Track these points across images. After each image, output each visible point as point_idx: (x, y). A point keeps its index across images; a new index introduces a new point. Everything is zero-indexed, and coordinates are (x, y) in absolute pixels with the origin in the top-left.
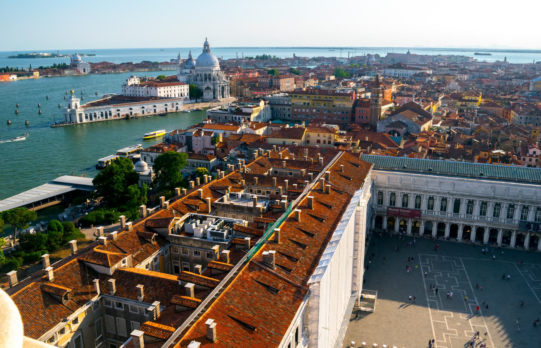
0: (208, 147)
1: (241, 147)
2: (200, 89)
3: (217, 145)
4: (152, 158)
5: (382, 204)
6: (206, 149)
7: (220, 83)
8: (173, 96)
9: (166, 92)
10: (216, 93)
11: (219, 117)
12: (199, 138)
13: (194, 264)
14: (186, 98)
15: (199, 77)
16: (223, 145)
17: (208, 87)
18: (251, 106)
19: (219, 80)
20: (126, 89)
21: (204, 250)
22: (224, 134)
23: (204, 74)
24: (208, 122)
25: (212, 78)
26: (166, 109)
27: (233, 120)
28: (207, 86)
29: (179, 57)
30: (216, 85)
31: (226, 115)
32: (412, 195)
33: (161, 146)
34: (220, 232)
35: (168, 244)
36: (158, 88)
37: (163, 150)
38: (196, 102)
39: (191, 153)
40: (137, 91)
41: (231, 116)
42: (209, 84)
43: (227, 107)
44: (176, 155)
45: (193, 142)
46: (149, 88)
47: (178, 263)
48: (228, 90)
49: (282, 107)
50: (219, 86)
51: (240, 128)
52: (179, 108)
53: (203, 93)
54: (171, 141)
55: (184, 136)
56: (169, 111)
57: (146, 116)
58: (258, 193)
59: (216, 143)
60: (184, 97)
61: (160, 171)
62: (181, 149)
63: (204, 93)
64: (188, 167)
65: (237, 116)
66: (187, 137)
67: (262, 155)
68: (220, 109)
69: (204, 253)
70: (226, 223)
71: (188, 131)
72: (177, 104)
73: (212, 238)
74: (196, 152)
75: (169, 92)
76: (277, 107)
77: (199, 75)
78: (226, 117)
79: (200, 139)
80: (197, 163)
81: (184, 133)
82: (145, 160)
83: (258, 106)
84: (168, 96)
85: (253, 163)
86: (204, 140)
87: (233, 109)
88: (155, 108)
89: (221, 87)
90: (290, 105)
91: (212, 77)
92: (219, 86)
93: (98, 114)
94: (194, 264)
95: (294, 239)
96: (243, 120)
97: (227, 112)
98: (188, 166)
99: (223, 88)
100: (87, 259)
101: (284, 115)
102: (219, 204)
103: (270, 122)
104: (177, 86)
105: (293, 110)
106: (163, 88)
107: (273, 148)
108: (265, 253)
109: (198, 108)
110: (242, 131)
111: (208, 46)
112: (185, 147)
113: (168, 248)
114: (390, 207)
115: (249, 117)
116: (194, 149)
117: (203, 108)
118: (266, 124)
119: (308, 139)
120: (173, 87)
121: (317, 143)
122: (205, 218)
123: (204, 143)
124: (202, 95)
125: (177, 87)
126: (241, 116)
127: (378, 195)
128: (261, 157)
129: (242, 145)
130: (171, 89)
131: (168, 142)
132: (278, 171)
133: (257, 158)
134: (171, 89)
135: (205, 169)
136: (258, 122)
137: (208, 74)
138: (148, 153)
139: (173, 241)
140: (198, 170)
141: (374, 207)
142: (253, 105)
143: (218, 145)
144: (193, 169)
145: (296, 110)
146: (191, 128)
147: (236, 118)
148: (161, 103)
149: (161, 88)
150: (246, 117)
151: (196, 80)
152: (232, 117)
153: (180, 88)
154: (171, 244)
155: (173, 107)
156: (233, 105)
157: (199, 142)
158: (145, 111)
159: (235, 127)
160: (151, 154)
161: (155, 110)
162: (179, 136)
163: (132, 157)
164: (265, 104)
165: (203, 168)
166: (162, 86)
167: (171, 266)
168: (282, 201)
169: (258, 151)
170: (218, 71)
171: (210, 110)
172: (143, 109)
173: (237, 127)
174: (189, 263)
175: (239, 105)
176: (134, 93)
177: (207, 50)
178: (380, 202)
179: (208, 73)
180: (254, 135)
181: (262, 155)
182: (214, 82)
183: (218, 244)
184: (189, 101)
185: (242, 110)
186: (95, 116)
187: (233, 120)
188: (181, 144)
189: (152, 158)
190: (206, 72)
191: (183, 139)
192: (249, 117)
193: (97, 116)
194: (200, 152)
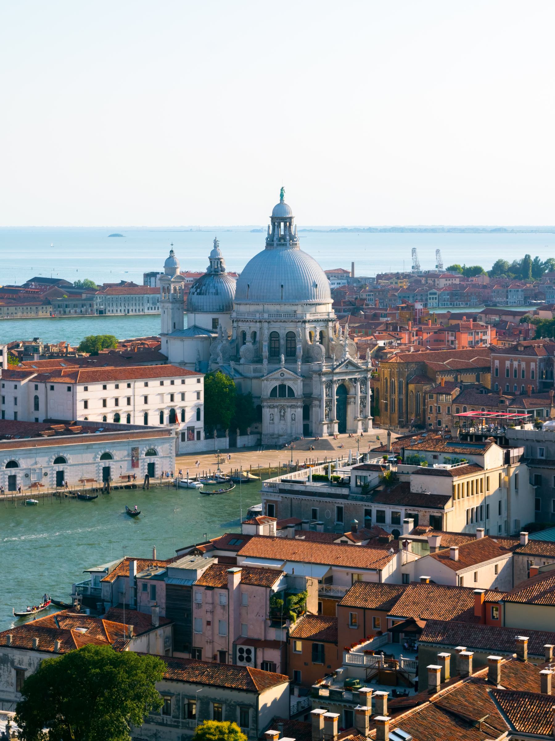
0: (256, 637)
1: (395, 640)
2: (249, 397)
3: (293, 626)
4: (20, 672)
7: (332, 373)
8: (138, 421)
9: (111, 403)
10: (314, 410)
11: (314, 512)
12: (222, 596)
14: (191, 429)
15: (249, 345)
16: (321, 626)
17: (282, 387)
18: (449, 467)
19: (329, 358)
22: (328, 580)
23: (266, 333)
24: (262, 530)
25: (300, 353)
26: (107, 471)
27: (368, 523)
28: (277, 384)
30: (315, 377)
31: (341, 502)
33: (63, 625)
36: (80, 389)
37: (69, 642)
38: (233, 447)
39: (186, 656)
41: (363, 505)
42: (289, 374)
43: (351, 467)
44: (116, 662)
45: (196, 613)
46: (41, 386)
48: (364, 399)
50: (329, 385)
51: (395, 558)
52: (158, 472)
53: (259, 409)
54: (107, 606)
55: (161, 587)
57: (25, 502)
59: (291, 619)
61: (46, 731)
62: (144, 639)
63: (266, 412)
64: (168, 719)
65: (388, 510)
66: (167, 585)
67: (464, 676)
68: (316, 478)
71: (174, 565)
72: (152, 453)
74: (207, 654)
75: (123, 402)
77: (249, 338)
78: (340, 510)
79: (224, 600)
80: (205, 702)
81: (160, 571)
83: (479, 467)
84: (117, 418)
85: (422, 706)
86: (240, 604)
87: (373, 477)
88: (60, 467)
89: (335, 387)
91: (299, 346)
92: (329, 385)
96: (411, 526)
97: (345, 491)
98: (166, 712)
99: (343, 390)
103: (526, 538)
104: (158, 383)
106: (100, 387)
107: (518, 647)
109: (236, 472)
110: (404, 570)
111: (288, 221)
112: (160, 631)
115: (436, 513)
116: (197, 641)
117: (254, 473)
118: (506, 544)
120: (139, 385)
123: (239, 616)
124: (259, 418)
125: (154, 384)
126: (402, 510)
128: (459, 684)
129: (396, 631)
130: (129, 392)
133: (444, 684)
134: (129, 392)
135: (235, 726)
136: (474, 536)
137: (283, 333)
138: (8, 651)
140: (207, 731)
142: (453, 462)
143: (300, 628)
144: (186, 726)
146: (192, 553)
147: (381, 517)
148: (88, 447)
149: (90, 387)
150: (425, 514)
151: (237, 359)
152: (368, 513)
153: (167, 388)
155: (134, 464)
156: (374, 462)
157: (219, 610)
158: (18, 479)
159: (375, 554)
160: (17, 656)
161: (60, 475)
162: (140, 585)
164: (507, 460)
165: (225, 725)
166: (94, 378)
169: (453, 659)
170: (327, 321)
171: (277, 480)
172: (13, 471)
173: (384, 553)
175: (395, 463)
177: (283, 238)
179: (283, 329)
180: (449, 587)
181: (464, 676)
182: (306, 367)
184: (202, 444)
185: (408, 484)
187: (368, 523)
188: (148, 618)
189: (20, 672)
190: (276, 327)
191: (154, 597)
192: (436, 513)
194: (223, 654)
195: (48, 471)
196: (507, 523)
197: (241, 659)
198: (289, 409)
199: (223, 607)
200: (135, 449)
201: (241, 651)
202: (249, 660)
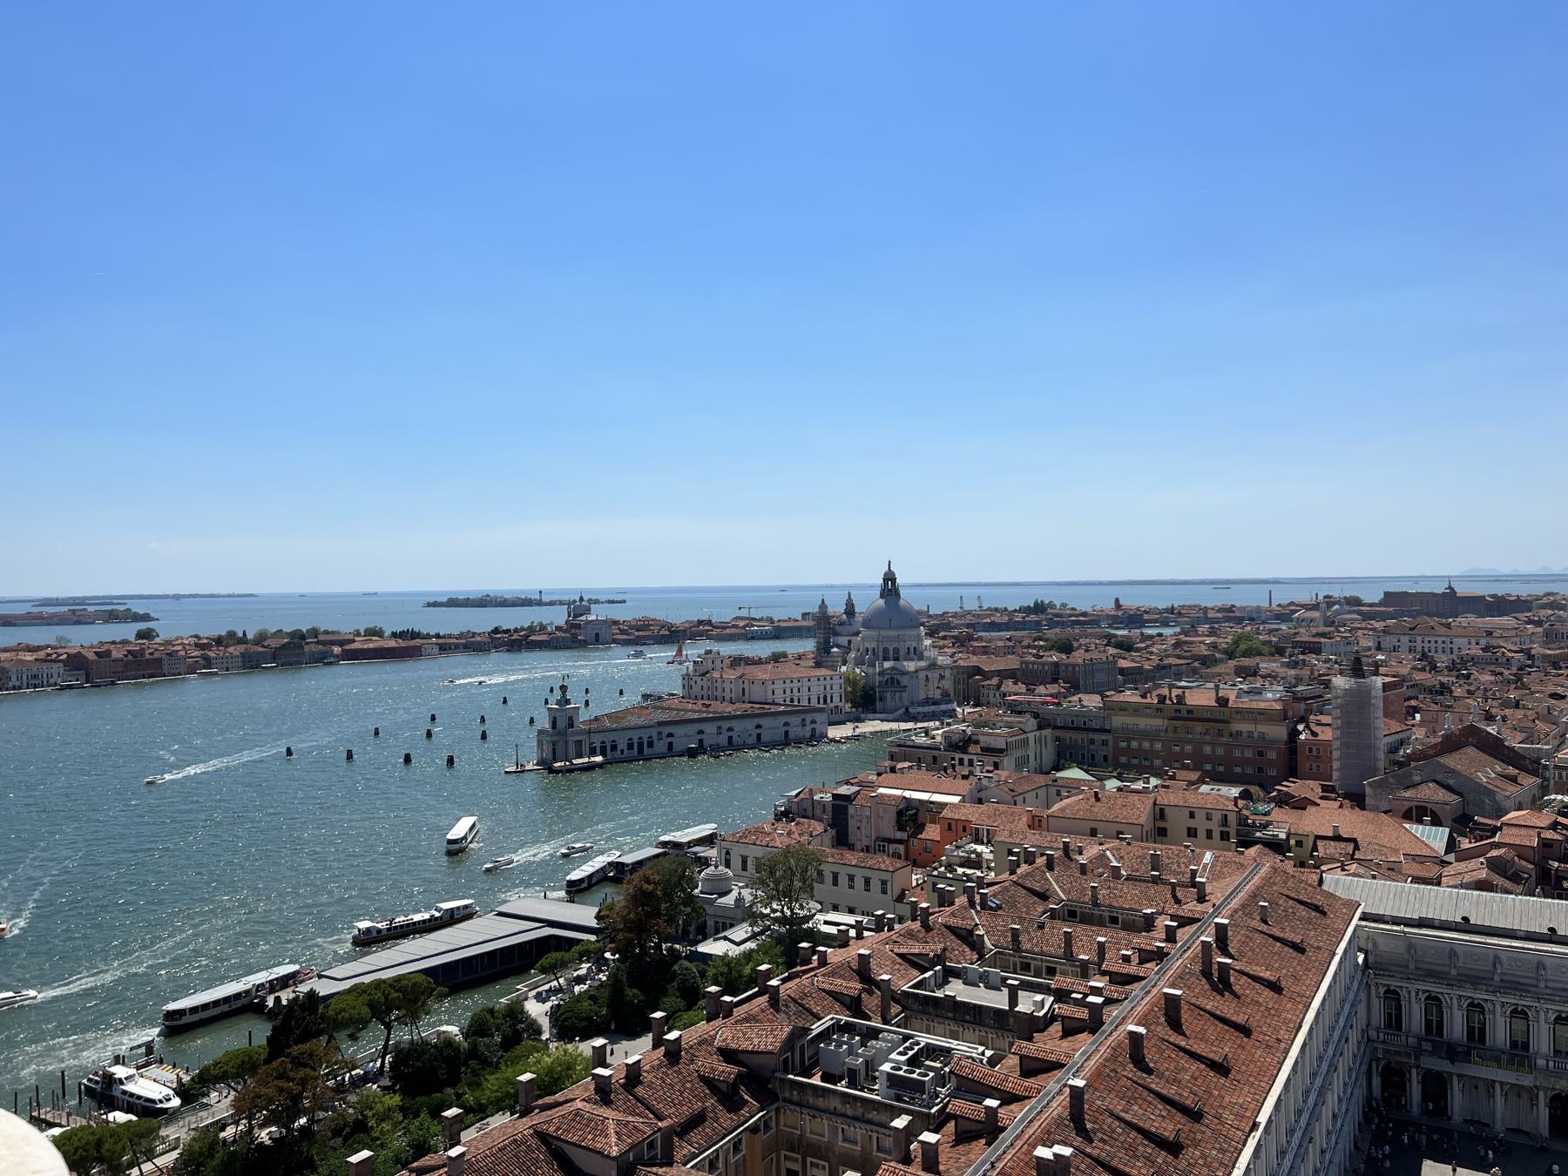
5: (1399, 1027)
6: (884, 840)
9: (788, 691)
13: (841, 1168)
14: (836, 707)
17: (892, 678)
20: (692, 683)
21: (869, 1127)
29: (823, 605)
31: (936, 753)
32: (1498, 1007)
34: (915, 1076)
35: (773, 1103)
40: (720, 689)
47: (796, 1160)
49: (1085, 736)
56: (791, 736)
58: (1022, 969)
60: (832, 705)
69: (870, 1136)
70: (931, 1052)
72: (813, 722)
73: (892, 1092)
75: (795, 690)
76: (1071, 735)
79: (868, 814)
82: (728, 865)
84: (792, 701)
88: (758, 731)
90: (1109, 731)
93: (622, 745)
94: (841, 1168)
95: (1128, 1117)
100: (558, 1129)
101: (1093, 756)
102: (914, 993)
105: (1116, 742)
108: (1043, 1152)
111: (894, 580)
113: (773, 1114)
114: (1426, 1040)
116: (852, 839)
119: (1161, 824)
121: (1189, 835)
122: (874, 1034)
127: (1385, 998)
131: (787, 817)
132: (1079, 910)
139: (787, 1094)
141: (1373, 1034)
145: (1123, 744)
147: (961, 762)
153: (822, 682)
154: (781, 1104)
161: (759, 735)
163: (695, 854)
167: (778, 1170)
168: (1091, 999)
174: (826, 1164)
176: (710, 693)
178: (1394, 1021)
183: (908, 1112)
186: (614, 748)
191: (824, 812)
193: (619, 750)
195: (752, 733)
196: (1041, 766)
197: (879, 851)
198: (897, 694)
199: (867, 817)
200: (804, 720)
201: (879, 845)
202: (884, 851)
